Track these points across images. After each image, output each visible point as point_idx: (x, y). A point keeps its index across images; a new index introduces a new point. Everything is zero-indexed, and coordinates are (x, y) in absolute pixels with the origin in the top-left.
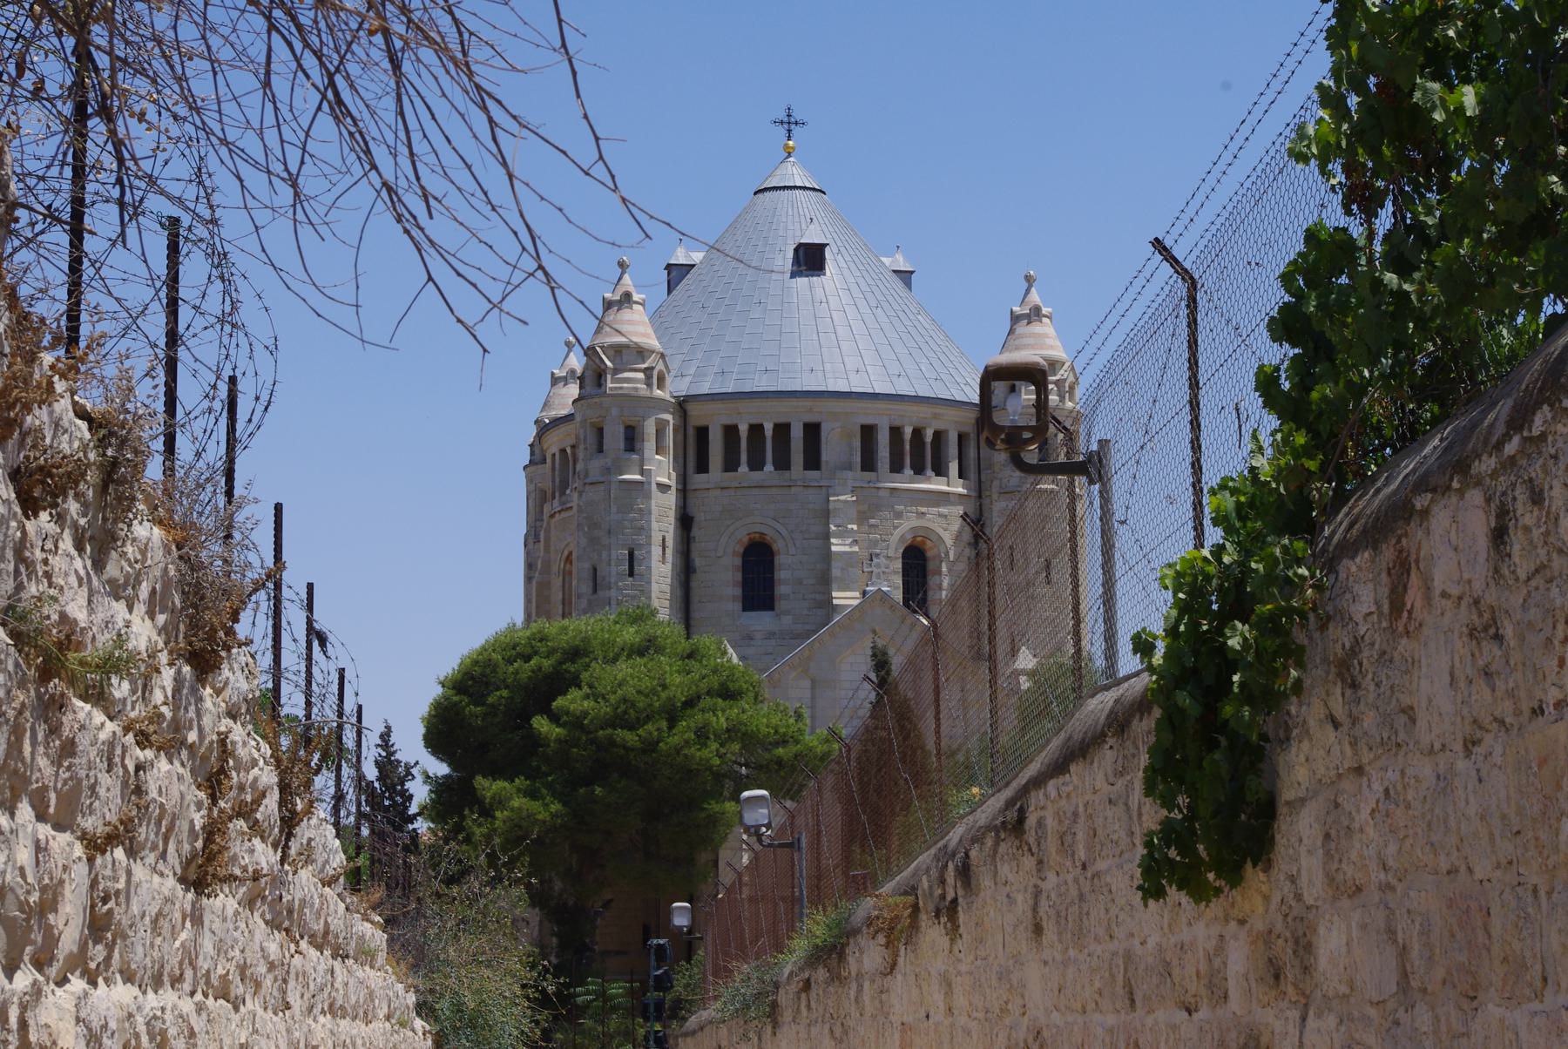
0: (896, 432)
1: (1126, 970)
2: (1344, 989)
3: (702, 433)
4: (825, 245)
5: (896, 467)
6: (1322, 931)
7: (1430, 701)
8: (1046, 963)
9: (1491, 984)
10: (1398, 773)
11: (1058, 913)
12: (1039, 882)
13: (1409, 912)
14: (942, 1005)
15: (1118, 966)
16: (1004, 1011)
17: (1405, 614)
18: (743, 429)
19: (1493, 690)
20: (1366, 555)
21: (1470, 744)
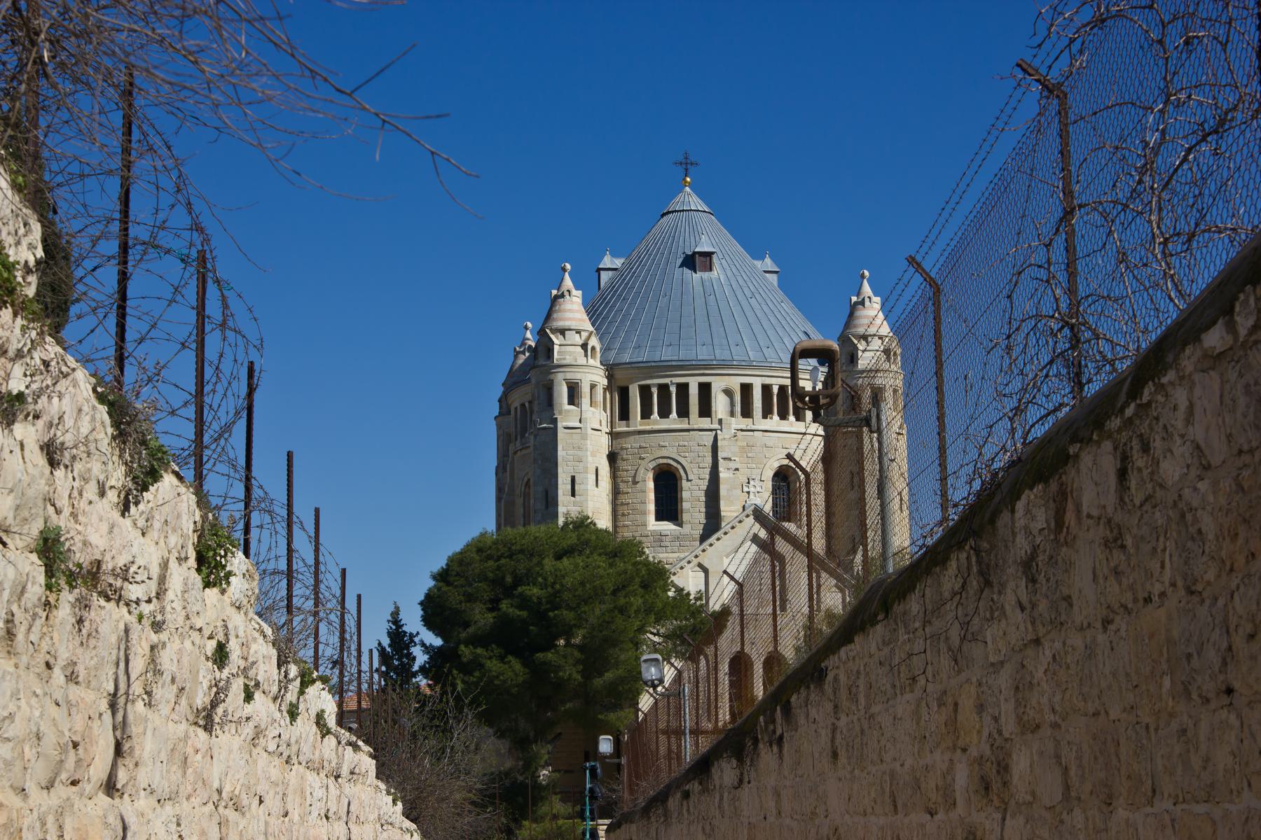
0: (766, 389)
1: (891, 784)
2: (1029, 798)
4: (713, 253)
5: (767, 413)
6: (1014, 757)
7: (1080, 592)
8: (840, 780)
9: (1120, 794)
10: (1061, 644)
11: (848, 745)
12: (836, 721)
13: (1069, 743)
14: (774, 811)
15: (886, 781)
16: (814, 814)
17: (1065, 530)
19: (1120, 585)
20: (1040, 487)
21: (1106, 622)
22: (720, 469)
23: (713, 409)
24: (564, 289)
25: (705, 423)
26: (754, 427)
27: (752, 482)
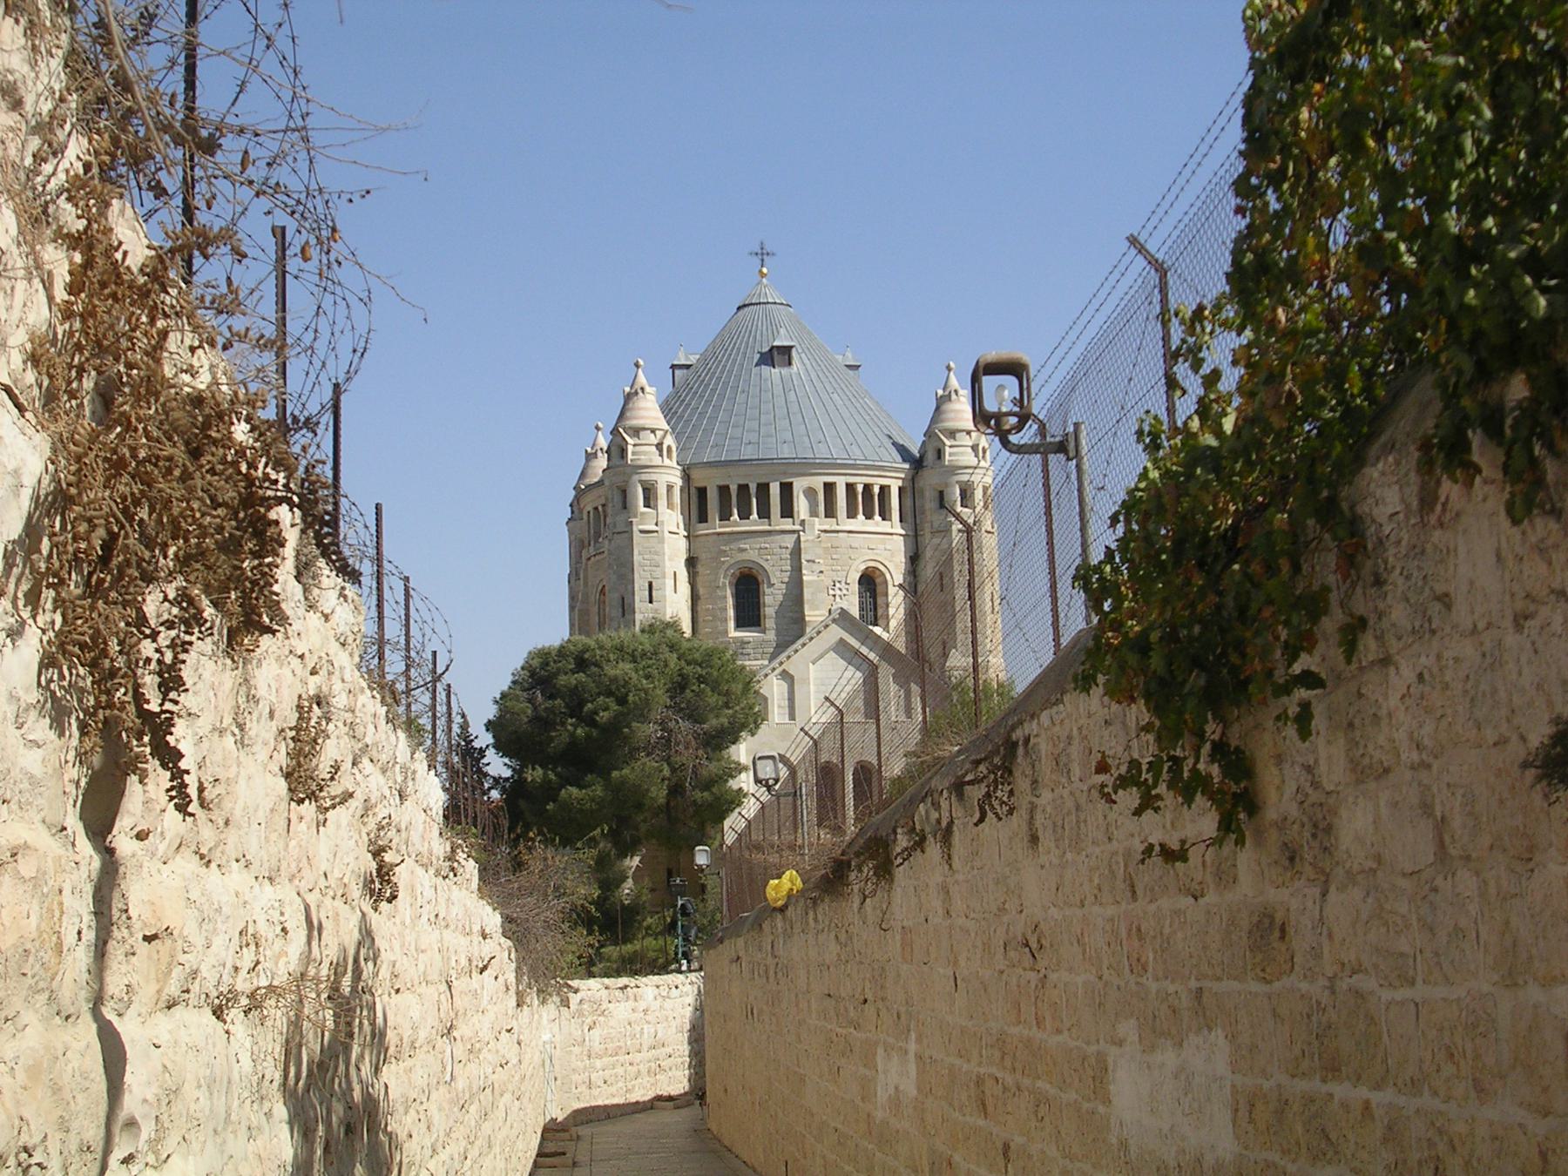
0: (850, 488)
1: (1126, 866)
2: (1372, 864)
3: (702, 492)
4: (792, 347)
5: (851, 514)
6: (1344, 813)
7: (1472, 583)
8: (1042, 867)
9: (1551, 845)
10: (1432, 658)
11: (1054, 824)
12: (1034, 799)
13: (1448, 785)
14: (940, 911)
15: (1117, 863)
16: (1002, 910)
17: (1439, 508)
18: (734, 489)
19: (1550, 564)
20: (1391, 459)
21: (1520, 620)
22: (804, 572)
23: (796, 509)
24: (637, 386)
25: (787, 524)
26: (838, 528)
27: (838, 585)
